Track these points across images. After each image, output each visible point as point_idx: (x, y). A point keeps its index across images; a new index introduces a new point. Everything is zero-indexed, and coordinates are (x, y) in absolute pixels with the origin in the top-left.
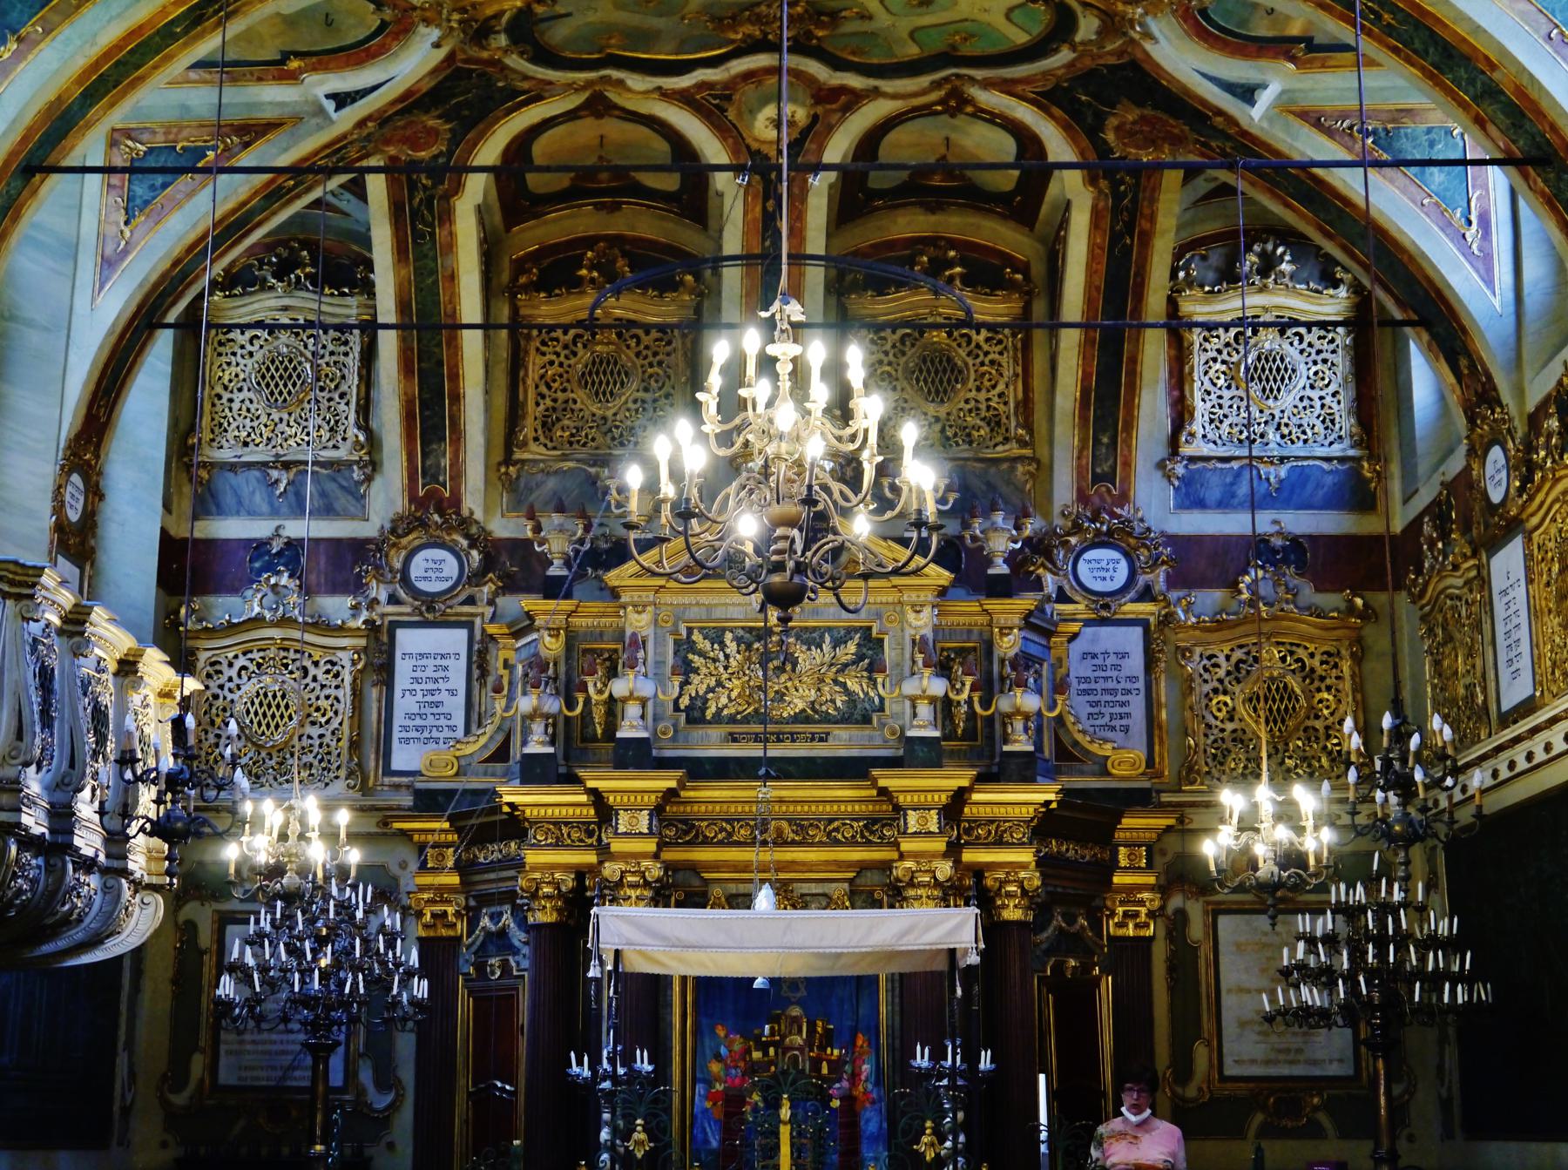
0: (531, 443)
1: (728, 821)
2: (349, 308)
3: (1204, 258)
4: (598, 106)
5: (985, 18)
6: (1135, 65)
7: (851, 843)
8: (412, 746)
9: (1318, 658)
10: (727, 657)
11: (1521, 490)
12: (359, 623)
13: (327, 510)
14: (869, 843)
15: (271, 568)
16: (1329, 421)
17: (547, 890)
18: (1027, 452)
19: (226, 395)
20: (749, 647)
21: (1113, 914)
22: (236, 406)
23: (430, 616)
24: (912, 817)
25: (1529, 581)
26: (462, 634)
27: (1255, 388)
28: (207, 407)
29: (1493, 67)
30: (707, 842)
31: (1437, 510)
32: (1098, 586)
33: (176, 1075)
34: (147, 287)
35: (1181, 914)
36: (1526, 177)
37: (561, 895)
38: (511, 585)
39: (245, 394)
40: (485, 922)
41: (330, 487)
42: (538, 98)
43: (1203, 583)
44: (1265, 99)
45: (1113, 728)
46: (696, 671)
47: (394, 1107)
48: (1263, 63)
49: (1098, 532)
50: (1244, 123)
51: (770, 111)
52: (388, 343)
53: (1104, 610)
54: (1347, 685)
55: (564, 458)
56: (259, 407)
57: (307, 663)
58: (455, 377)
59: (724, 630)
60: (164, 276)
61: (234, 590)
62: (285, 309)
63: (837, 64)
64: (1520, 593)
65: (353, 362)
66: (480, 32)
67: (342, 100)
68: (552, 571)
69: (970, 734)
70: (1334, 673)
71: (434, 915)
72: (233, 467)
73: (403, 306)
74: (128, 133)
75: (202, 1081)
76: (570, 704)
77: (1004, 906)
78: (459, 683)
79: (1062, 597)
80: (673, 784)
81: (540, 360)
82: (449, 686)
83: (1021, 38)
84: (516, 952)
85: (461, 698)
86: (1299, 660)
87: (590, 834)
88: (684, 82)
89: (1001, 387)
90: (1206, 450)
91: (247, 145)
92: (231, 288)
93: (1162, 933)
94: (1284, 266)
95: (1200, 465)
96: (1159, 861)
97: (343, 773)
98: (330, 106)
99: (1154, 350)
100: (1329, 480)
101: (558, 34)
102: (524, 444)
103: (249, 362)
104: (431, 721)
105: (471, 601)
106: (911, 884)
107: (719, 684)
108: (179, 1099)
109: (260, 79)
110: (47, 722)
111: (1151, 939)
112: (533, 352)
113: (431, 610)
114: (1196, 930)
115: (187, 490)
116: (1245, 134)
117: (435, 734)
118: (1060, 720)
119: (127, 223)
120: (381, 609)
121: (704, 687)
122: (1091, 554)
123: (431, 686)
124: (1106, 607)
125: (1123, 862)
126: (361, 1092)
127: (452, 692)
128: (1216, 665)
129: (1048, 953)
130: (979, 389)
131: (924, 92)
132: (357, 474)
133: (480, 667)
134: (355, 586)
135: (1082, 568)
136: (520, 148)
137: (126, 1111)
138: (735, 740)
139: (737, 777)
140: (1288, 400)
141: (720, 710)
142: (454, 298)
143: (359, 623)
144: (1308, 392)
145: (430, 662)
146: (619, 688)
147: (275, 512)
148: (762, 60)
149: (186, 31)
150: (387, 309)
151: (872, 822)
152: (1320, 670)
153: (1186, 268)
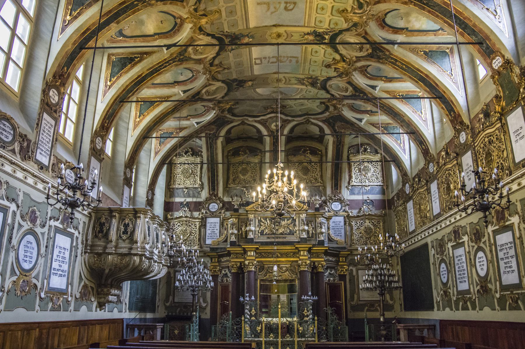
2: (198, 160)
3: (354, 149)
4: (243, 123)
5: (313, 107)
6: (340, 115)
7: (290, 257)
8: (210, 239)
11: (412, 191)
12: (200, 217)
13: (194, 196)
14: (294, 257)
15: (184, 207)
16: (377, 178)
17: (235, 266)
21: (339, 270)
24: (302, 252)
25: (414, 208)
26: (219, 219)
27: (364, 173)
28: (172, 178)
29: (404, 117)
30: (264, 257)
31: (398, 195)
32: (335, 209)
33: (167, 300)
35: (352, 270)
36: (410, 136)
37: (237, 267)
38: (227, 210)
39: (179, 175)
40: (223, 272)
42: (233, 122)
43: (355, 209)
44: (364, 121)
46: (262, 226)
48: (363, 115)
49: (335, 199)
50: (360, 126)
51: (274, 124)
52: (205, 166)
53: (336, 213)
54: (382, 227)
55: (237, 186)
56: (182, 177)
57: (191, 224)
58: (217, 172)
59: (267, 218)
61: (177, 211)
62: (187, 160)
63: (286, 115)
64: (412, 210)
65: (199, 169)
66: (223, 111)
67: (197, 123)
68: (235, 207)
69: (312, 237)
71: (214, 271)
72: (177, 189)
73: (208, 160)
75: (171, 301)
76: (239, 231)
77: (319, 269)
78: (218, 227)
79: (329, 211)
80: (258, 246)
81: (233, 169)
83: (320, 111)
84: (229, 277)
85: (218, 231)
86: (373, 223)
87: (243, 256)
89: (317, 173)
90: (355, 184)
91: (181, 131)
93: (348, 273)
95: (354, 187)
97: (197, 244)
98: (195, 124)
99: (345, 166)
100: (378, 189)
101: (236, 111)
102: (230, 184)
104: (213, 235)
106: (301, 265)
108: (168, 304)
110: (149, 236)
111: (346, 275)
113: (213, 215)
114: (354, 273)
115: (169, 193)
116: (360, 127)
118: (329, 234)
122: (334, 203)
125: (341, 260)
126: (200, 303)
127: (217, 230)
129: (327, 277)
131: (302, 120)
132: (199, 190)
134: (199, 210)
135: (332, 206)
136: (229, 132)
137: (158, 306)
139: (270, 245)
140: (369, 174)
141: (266, 233)
142: (217, 158)
143: (200, 217)
144: (373, 173)
145: (213, 224)
146: (248, 229)
147: (185, 197)
149: (172, 113)
150: (205, 160)
151: (294, 253)
152: (377, 224)
153: (351, 151)
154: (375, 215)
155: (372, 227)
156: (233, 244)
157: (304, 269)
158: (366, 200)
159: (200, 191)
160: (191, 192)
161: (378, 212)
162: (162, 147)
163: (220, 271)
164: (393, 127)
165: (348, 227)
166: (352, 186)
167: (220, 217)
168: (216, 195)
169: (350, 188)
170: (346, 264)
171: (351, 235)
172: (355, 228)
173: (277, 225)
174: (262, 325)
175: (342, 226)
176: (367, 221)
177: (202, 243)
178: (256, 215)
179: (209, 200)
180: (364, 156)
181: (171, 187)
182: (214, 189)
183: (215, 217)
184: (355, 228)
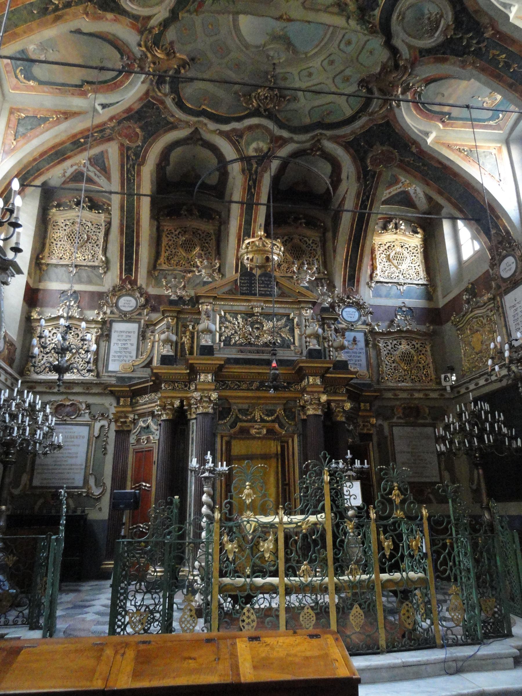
0: (163, 264)
1: (239, 381)
2: (102, 217)
8: (116, 362)
9: (419, 345)
10: (238, 323)
12: (99, 319)
13: (90, 282)
16: (418, 273)
18: (326, 277)
19: (55, 242)
20: (246, 320)
22: (58, 246)
23: (125, 319)
27: (395, 262)
28: (47, 245)
30: (231, 389)
32: (349, 319)
34: (21, 166)
39: (62, 242)
40: (141, 424)
41: (91, 274)
45: (356, 364)
47: (102, 493)
49: (349, 303)
51: (254, 145)
54: (429, 353)
58: (138, 237)
60: (30, 163)
61: (53, 307)
63: (281, 126)
67: (104, 106)
70: (424, 349)
72: (56, 266)
74: (19, 110)
75: (25, 485)
77: (338, 416)
78: (134, 341)
81: (166, 239)
82: (131, 342)
84: (153, 434)
85: (135, 347)
87: (186, 386)
88: (226, 128)
89: (317, 257)
90: (382, 280)
92: (59, 207)
93: (375, 433)
94: (403, 227)
95: (379, 284)
96: (373, 408)
98: (99, 108)
100: (418, 291)
102: (160, 264)
103: (63, 231)
104: (124, 354)
105: (140, 314)
107: (236, 332)
109: (73, 94)
112: (164, 236)
117: (125, 358)
119: (15, 140)
120: (107, 316)
121: (230, 334)
122: (347, 309)
123: (124, 342)
124: (352, 326)
125: (362, 408)
127: (132, 345)
128: (388, 346)
130: (310, 257)
132: (101, 271)
133: (142, 336)
134: (100, 308)
138: (242, 352)
140: (404, 267)
141: (236, 342)
143: (99, 319)
144: (411, 265)
145: (124, 334)
146: (201, 327)
148: (254, 121)
152: (420, 349)
154: (418, 333)
155: (413, 351)
156: (165, 360)
157: (317, 413)
158: (400, 308)
159: (101, 274)
160: (84, 274)
161: (423, 328)
162: (20, 144)
163: (134, 422)
164: (484, 152)
165: (371, 350)
166: (377, 282)
167: (139, 322)
168: (133, 283)
169: (373, 285)
170: (371, 414)
171: (378, 366)
172: (384, 353)
173: (258, 328)
174: (275, 534)
175: (362, 349)
176: (403, 342)
177: (100, 368)
178: (217, 308)
179: (119, 290)
180: (395, 237)
181: (43, 261)
182: (129, 270)
183: (130, 321)
184: (385, 353)
